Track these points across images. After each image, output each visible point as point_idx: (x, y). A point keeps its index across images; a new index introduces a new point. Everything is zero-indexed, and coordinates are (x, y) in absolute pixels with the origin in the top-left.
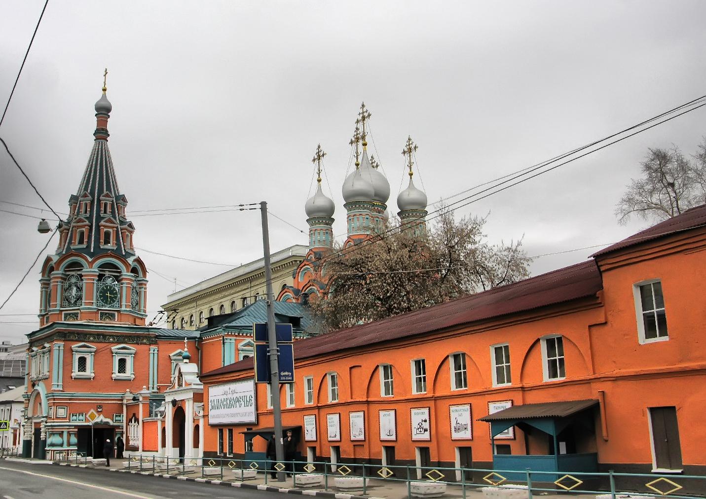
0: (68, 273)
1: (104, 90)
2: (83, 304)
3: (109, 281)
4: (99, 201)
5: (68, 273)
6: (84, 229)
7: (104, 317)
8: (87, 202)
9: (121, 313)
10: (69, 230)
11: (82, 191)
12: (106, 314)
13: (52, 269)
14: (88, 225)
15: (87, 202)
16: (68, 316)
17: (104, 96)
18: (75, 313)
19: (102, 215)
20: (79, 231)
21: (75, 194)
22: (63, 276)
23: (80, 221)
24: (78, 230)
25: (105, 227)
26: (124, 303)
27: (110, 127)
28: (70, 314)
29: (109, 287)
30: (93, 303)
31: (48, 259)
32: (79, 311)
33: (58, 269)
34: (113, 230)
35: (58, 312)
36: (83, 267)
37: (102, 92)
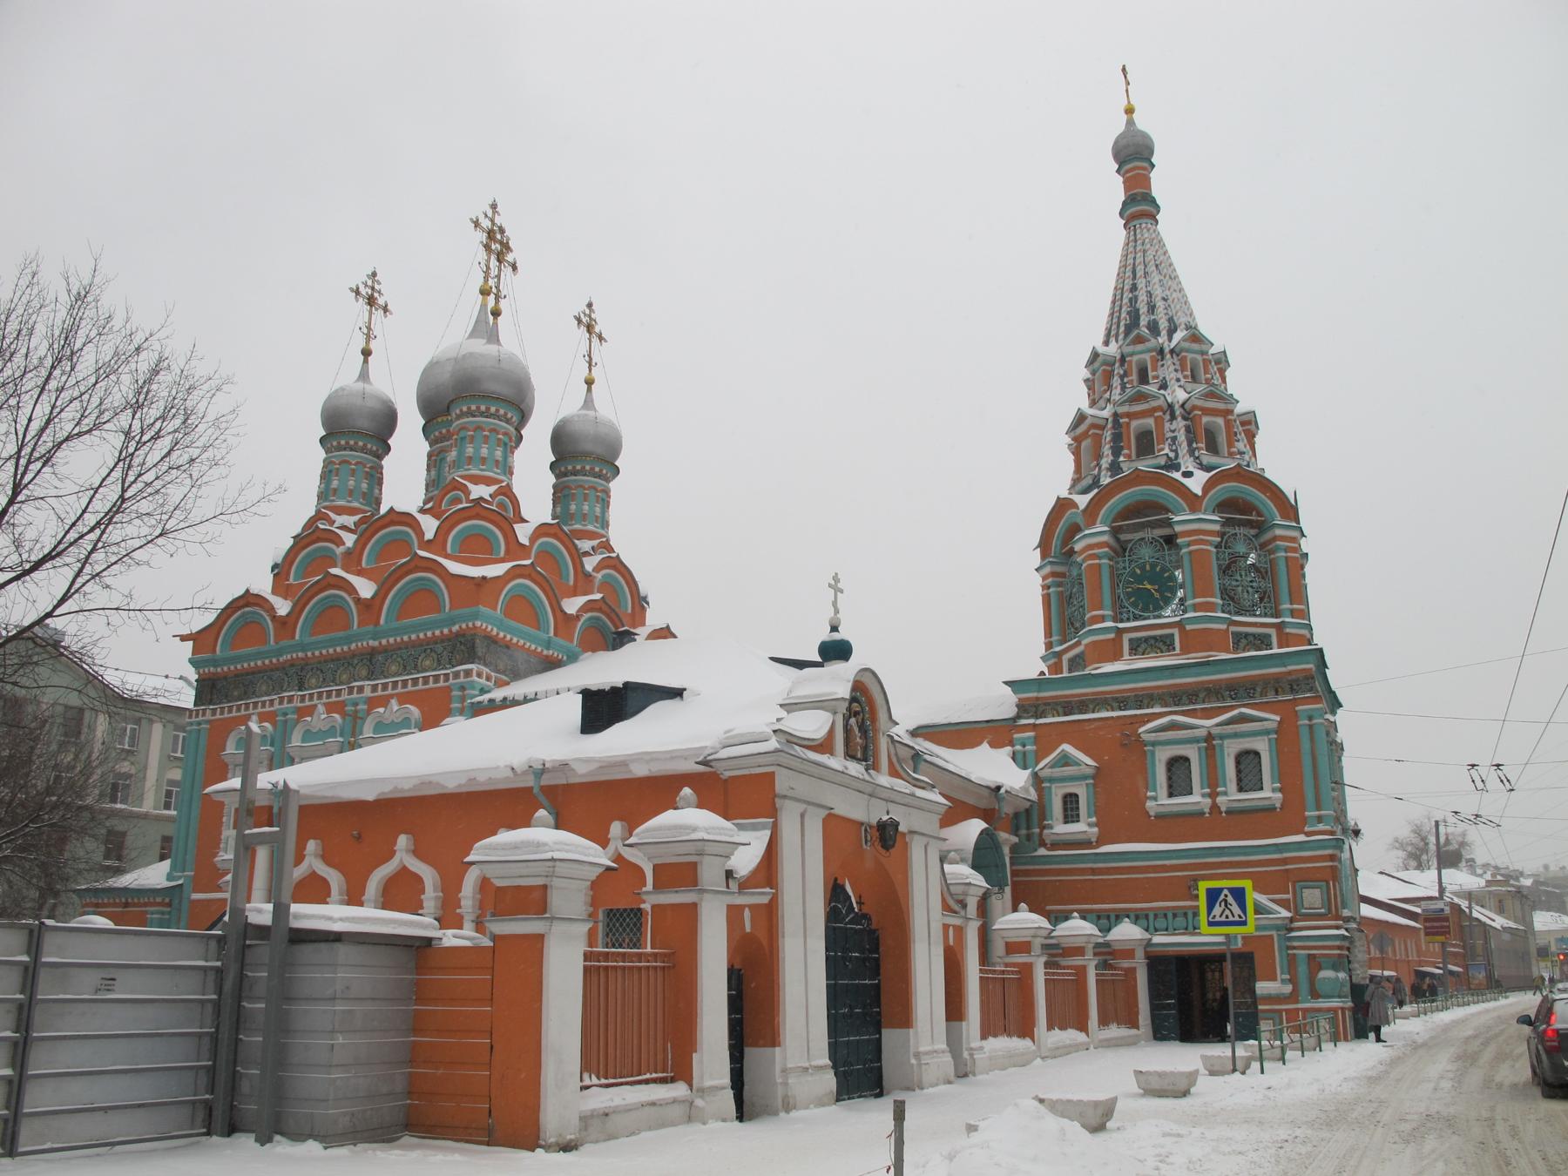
0: (1123, 537)
1: (1130, 111)
2: (1188, 609)
5: (1123, 537)
7: (1242, 645)
9: (1288, 630)
12: (1247, 635)
13: (1074, 529)
16: (1143, 646)
17: (1130, 123)
18: (1161, 636)
22: (1112, 541)
23: (1140, 397)
24: (1135, 424)
25: (1207, 411)
26: (1286, 606)
27: (1160, 185)
28: (1146, 640)
30: (1213, 603)
31: (1062, 506)
32: (1176, 631)
33: (1092, 523)
34: (1228, 424)
35: (1112, 636)
36: (1168, 511)
37: (1125, 117)
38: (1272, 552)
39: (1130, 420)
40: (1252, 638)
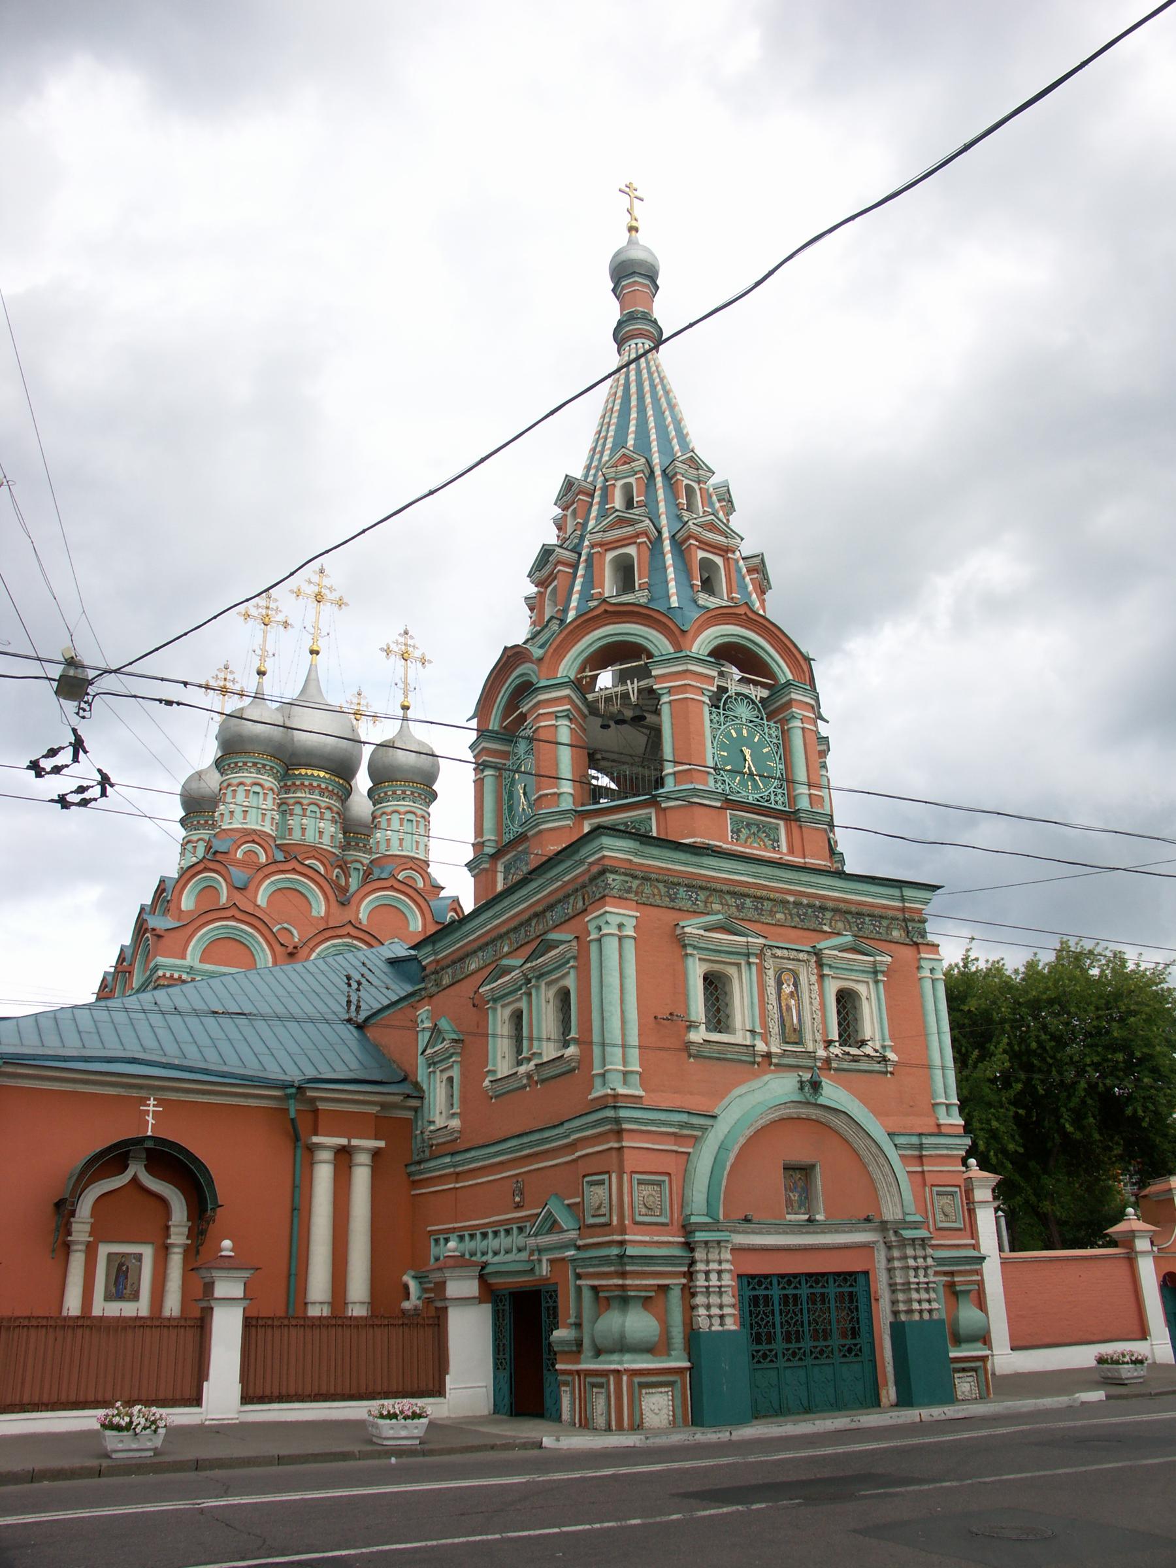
3: (744, 711)
4: (668, 476)
6: (632, 550)
7: (743, 835)
8: (632, 480)
10: (575, 566)
11: (607, 453)
12: (748, 825)
14: (645, 534)
15: (632, 480)
19: (686, 515)
20: (616, 560)
21: (578, 473)
23: (622, 522)
24: (610, 556)
29: (745, 732)
31: (512, 657)
38: (785, 721)
39: (606, 550)
40: (754, 829)
